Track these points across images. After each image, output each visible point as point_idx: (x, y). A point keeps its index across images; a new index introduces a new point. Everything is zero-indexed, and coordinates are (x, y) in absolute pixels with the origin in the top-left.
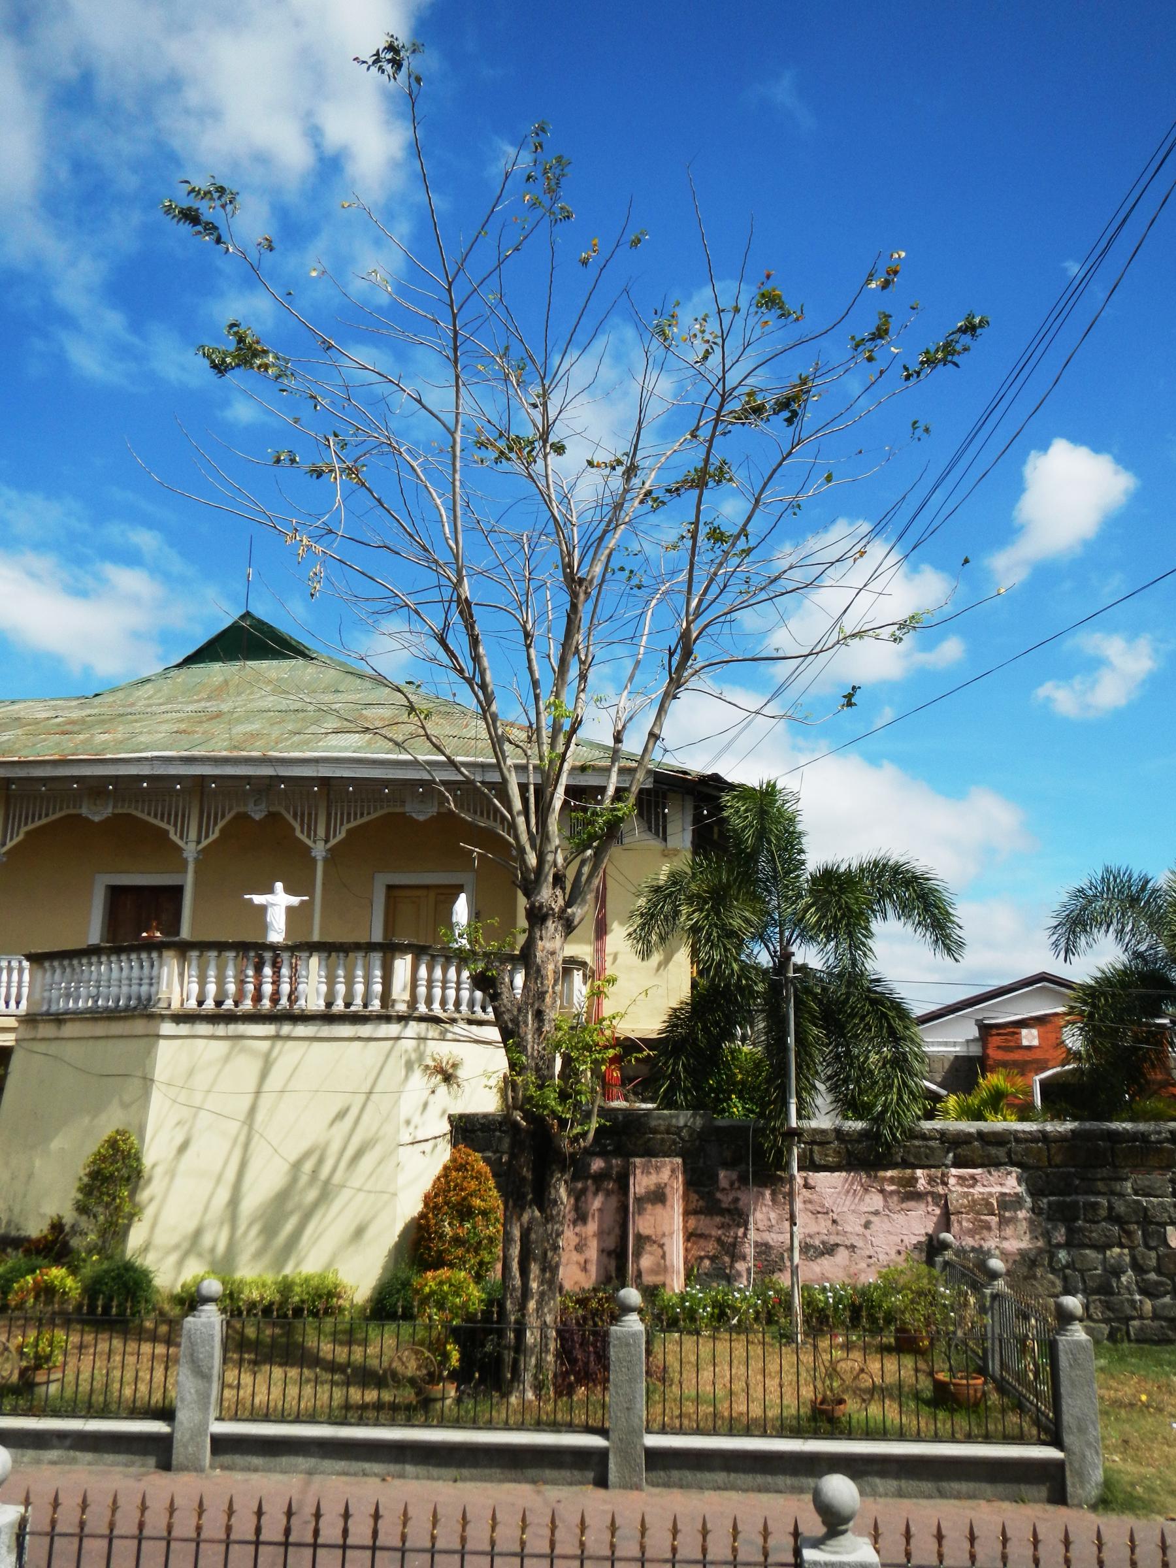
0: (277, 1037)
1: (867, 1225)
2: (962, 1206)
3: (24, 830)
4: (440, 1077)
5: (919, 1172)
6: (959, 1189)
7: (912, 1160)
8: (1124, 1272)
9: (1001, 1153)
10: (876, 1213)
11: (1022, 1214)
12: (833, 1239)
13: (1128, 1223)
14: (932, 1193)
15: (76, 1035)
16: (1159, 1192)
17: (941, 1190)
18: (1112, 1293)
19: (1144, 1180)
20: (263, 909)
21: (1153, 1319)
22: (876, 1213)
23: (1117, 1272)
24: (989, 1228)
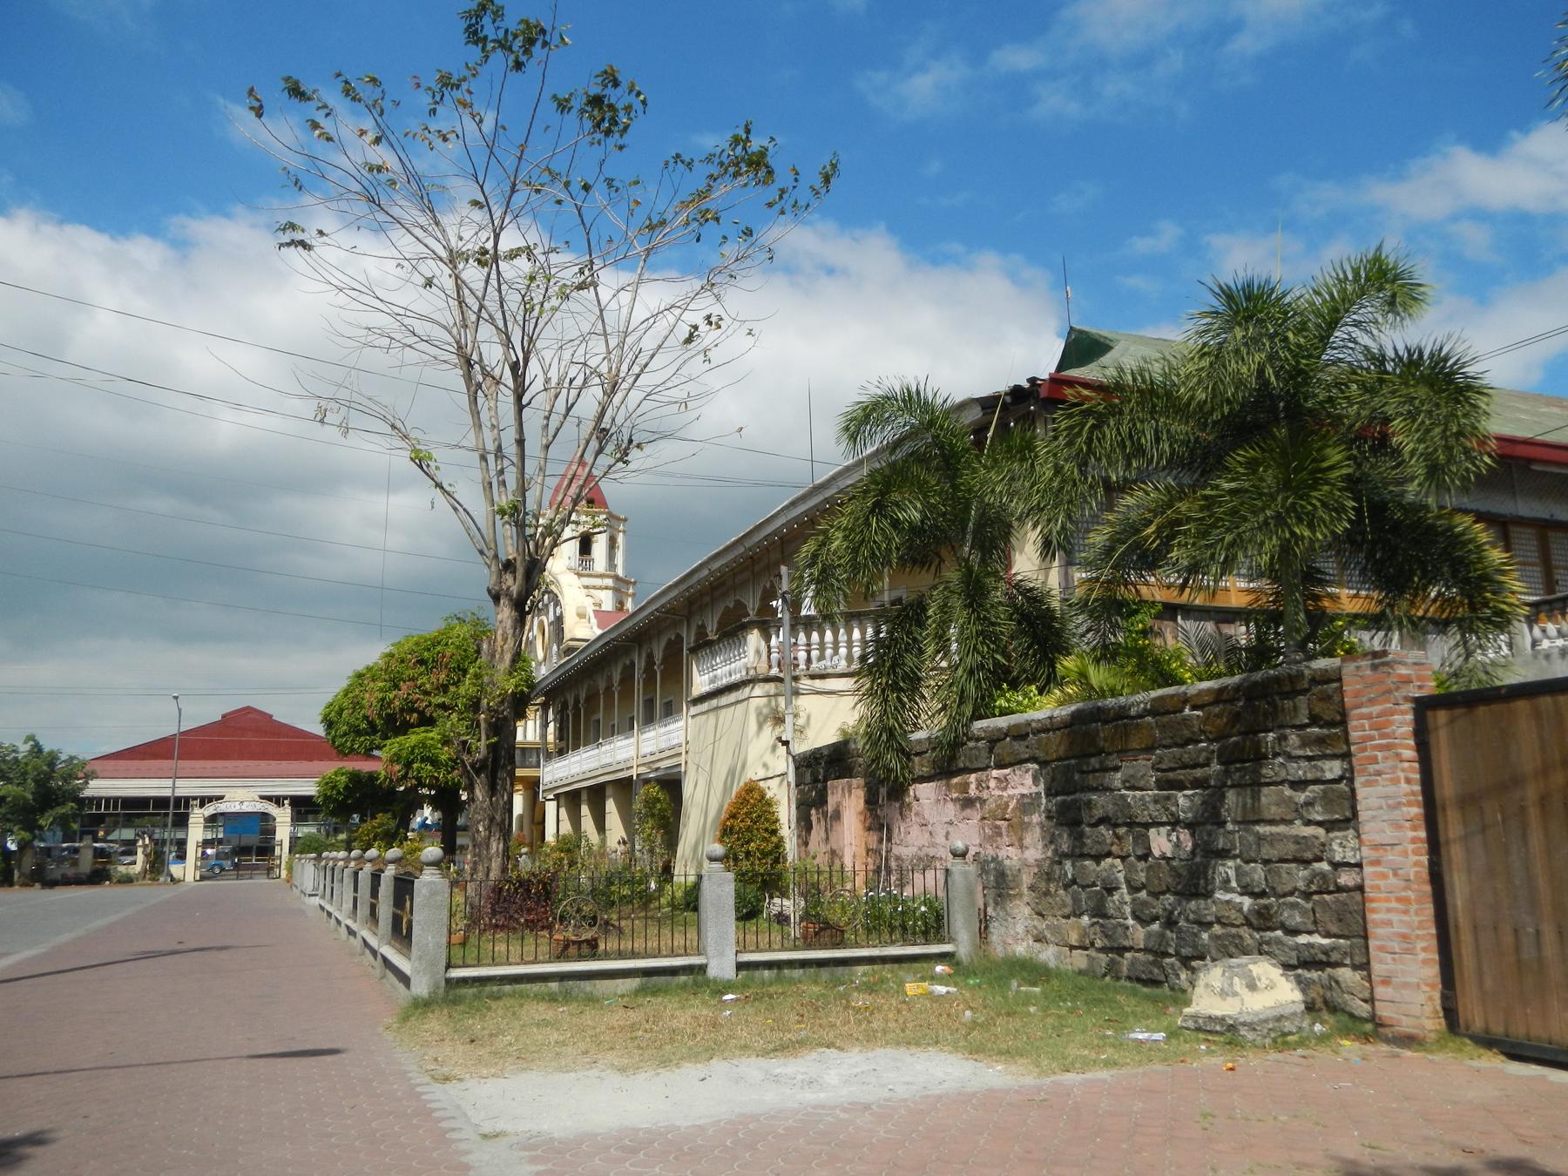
0: (718, 708)
5: (973, 776)
6: (997, 793)
8: (1116, 888)
9: (1019, 747)
11: (1036, 818)
13: (1116, 825)
14: (979, 798)
16: (1142, 783)
17: (985, 795)
18: (1105, 916)
19: (1128, 768)
21: (1146, 950)
22: (951, 823)
23: (1110, 890)
24: (1000, 835)
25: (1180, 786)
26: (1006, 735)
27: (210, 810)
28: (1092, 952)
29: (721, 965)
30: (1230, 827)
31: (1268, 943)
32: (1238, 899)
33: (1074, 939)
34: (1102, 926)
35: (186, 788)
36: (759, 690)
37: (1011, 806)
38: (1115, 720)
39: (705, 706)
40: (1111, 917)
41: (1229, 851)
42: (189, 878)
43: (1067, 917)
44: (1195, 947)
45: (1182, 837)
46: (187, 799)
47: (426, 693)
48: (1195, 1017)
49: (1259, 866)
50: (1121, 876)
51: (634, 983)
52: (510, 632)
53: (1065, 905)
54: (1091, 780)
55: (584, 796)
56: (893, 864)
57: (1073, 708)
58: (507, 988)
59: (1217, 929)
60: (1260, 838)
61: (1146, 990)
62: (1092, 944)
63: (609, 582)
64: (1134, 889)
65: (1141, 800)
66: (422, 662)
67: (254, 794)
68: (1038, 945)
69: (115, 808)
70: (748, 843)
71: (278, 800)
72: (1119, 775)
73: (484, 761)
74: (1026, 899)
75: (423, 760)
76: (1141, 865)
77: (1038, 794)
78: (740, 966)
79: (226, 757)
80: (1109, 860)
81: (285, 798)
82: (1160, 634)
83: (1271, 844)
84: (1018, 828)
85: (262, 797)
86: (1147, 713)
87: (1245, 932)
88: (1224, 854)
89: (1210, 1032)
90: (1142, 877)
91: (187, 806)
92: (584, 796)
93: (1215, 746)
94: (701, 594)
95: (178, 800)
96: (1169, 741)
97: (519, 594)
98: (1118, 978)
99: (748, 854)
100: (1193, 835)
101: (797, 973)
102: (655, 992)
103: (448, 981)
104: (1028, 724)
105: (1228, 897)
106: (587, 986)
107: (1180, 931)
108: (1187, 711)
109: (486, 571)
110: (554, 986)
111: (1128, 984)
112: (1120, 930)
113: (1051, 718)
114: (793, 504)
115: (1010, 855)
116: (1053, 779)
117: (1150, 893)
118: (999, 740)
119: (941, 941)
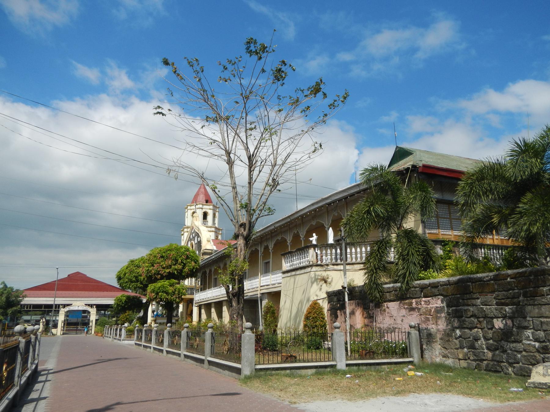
0: (295, 275)
1: (402, 321)
2: (423, 312)
4: (323, 282)
5: (414, 301)
6: (425, 306)
7: (411, 296)
8: (480, 339)
9: (435, 291)
10: (404, 316)
11: (443, 315)
12: (395, 326)
13: (479, 318)
14: (417, 308)
16: (490, 304)
17: (420, 306)
18: (475, 349)
20: (312, 241)
21: (492, 360)
22: (404, 316)
23: (477, 339)
24: (429, 321)
25: (507, 305)
26: (429, 286)
27: (67, 309)
28: (469, 361)
29: (341, 364)
30: (528, 319)
31: (547, 358)
32: (533, 343)
33: (461, 356)
34: (473, 352)
35: (59, 301)
36: (314, 269)
37: (433, 310)
38: (477, 282)
39: (289, 274)
40: (478, 349)
41: (528, 327)
42: (59, 334)
43: (458, 349)
44: (515, 359)
45: (508, 322)
46: (59, 305)
47: (164, 268)
48: (534, 383)
49: (542, 333)
50: (481, 335)
51: (314, 371)
52: (243, 248)
53: (456, 345)
54: (470, 302)
55: (213, 305)
56: (378, 331)
57: (458, 277)
58: (273, 372)
59: (524, 353)
60: (542, 323)
61: (495, 374)
62: (469, 358)
63: (213, 229)
64: (486, 339)
65: (491, 309)
66: (162, 257)
67: (83, 303)
68: (444, 359)
69: (30, 308)
70: (316, 322)
71: (91, 306)
72: (479, 301)
73: (236, 293)
74: (439, 343)
75: (163, 292)
76: (490, 331)
77: (444, 307)
78: (347, 365)
79: (71, 290)
80: (476, 330)
81: (94, 305)
82: (454, 252)
83: (547, 325)
84: (437, 318)
85: (86, 305)
86: (491, 280)
87: (537, 354)
88: (526, 328)
89: (542, 388)
90: (491, 335)
91: (59, 308)
92: (213, 305)
93: (522, 291)
95: (56, 305)
96: (501, 289)
97: (247, 235)
98: (480, 370)
99: (316, 326)
100: (513, 321)
101: (364, 368)
102: (320, 374)
103: (256, 369)
104: (438, 282)
105: (529, 342)
106: (299, 371)
107: (508, 353)
108: (509, 279)
109: (233, 227)
110: (288, 371)
111: (485, 372)
112: (481, 353)
113: (448, 281)
114: (313, 204)
115: (432, 327)
116: (450, 302)
117: (494, 341)
118: (425, 288)
119: (408, 357)
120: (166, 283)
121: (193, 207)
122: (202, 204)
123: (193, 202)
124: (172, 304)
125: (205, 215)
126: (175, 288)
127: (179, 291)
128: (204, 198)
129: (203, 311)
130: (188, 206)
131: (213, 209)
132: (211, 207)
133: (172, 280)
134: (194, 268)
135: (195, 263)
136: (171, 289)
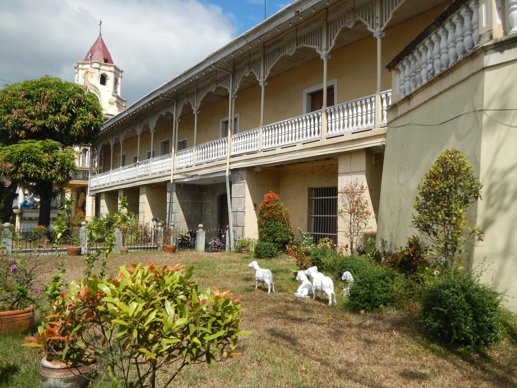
3: (392, 12)
15: (420, 102)
47: (32, 117)
55: (121, 194)
66: (28, 97)
75: (28, 162)
94: (250, 54)
120: (38, 144)
121: (88, 66)
122: (100, 63)
123: (86, 59)
124: (50, 185)
125: (103, 80)
126: (54, 155)
127: (63, 163)
128: (102, 56)
129: (103, 203)
130: (78, 64)
131: (114, 72)
132: (112, 69)
133: (49, 140)
134: (91, 124)
135: (95, 115)
136: (46, 158)
